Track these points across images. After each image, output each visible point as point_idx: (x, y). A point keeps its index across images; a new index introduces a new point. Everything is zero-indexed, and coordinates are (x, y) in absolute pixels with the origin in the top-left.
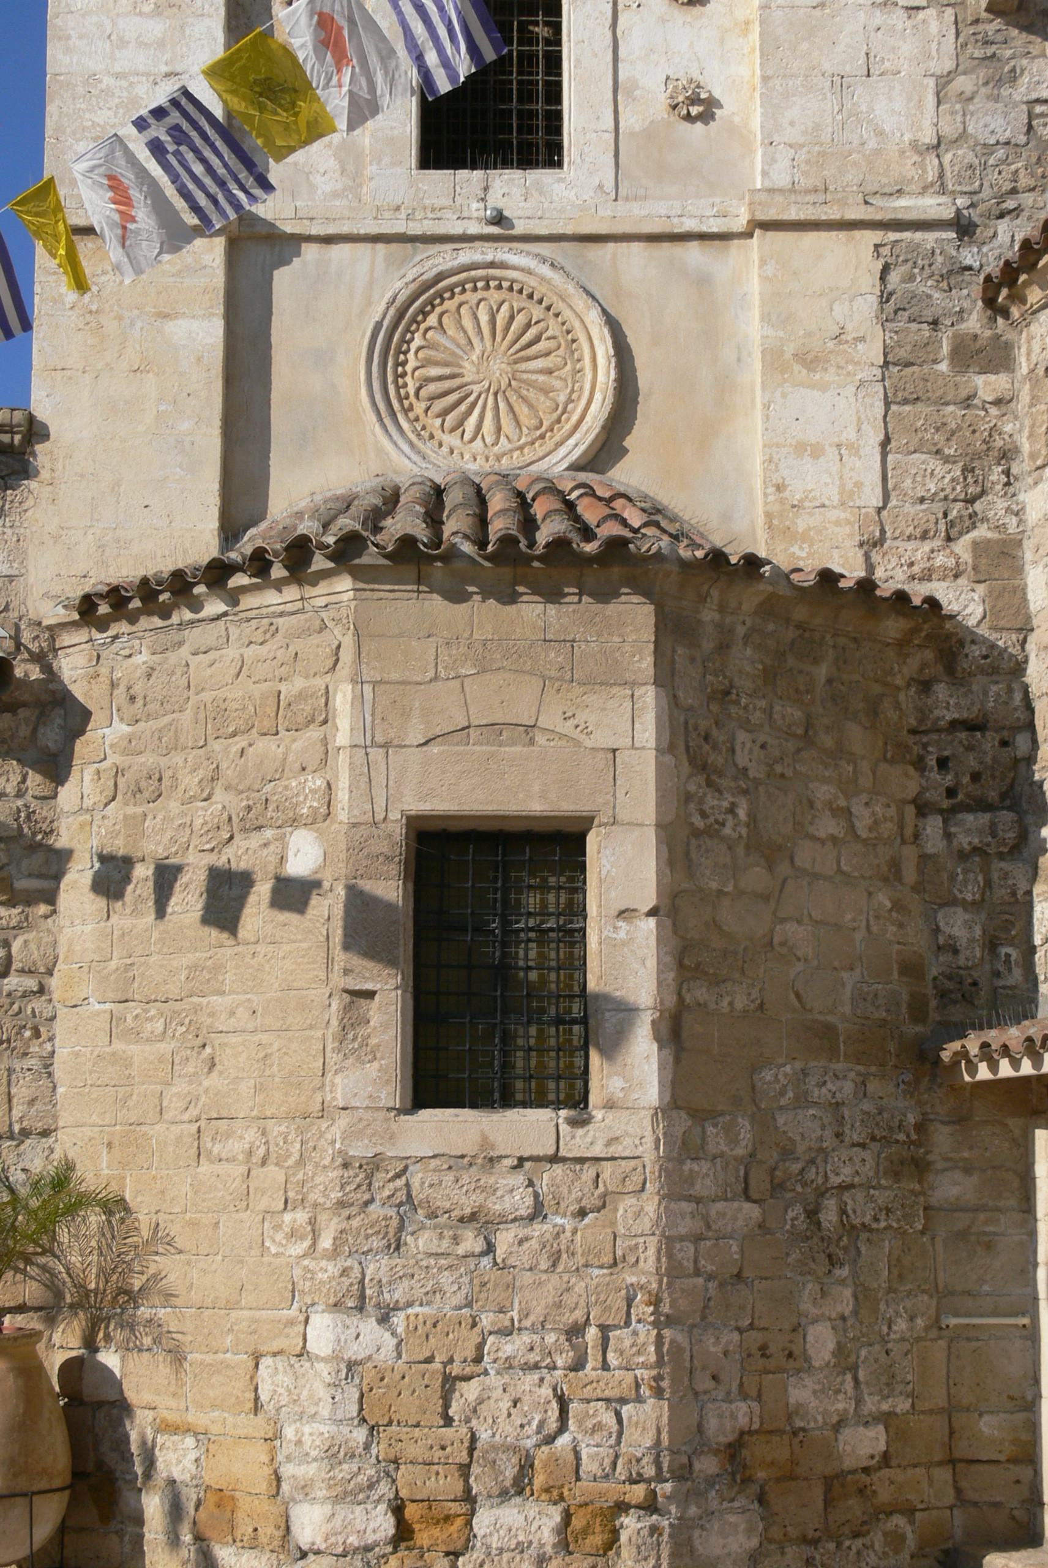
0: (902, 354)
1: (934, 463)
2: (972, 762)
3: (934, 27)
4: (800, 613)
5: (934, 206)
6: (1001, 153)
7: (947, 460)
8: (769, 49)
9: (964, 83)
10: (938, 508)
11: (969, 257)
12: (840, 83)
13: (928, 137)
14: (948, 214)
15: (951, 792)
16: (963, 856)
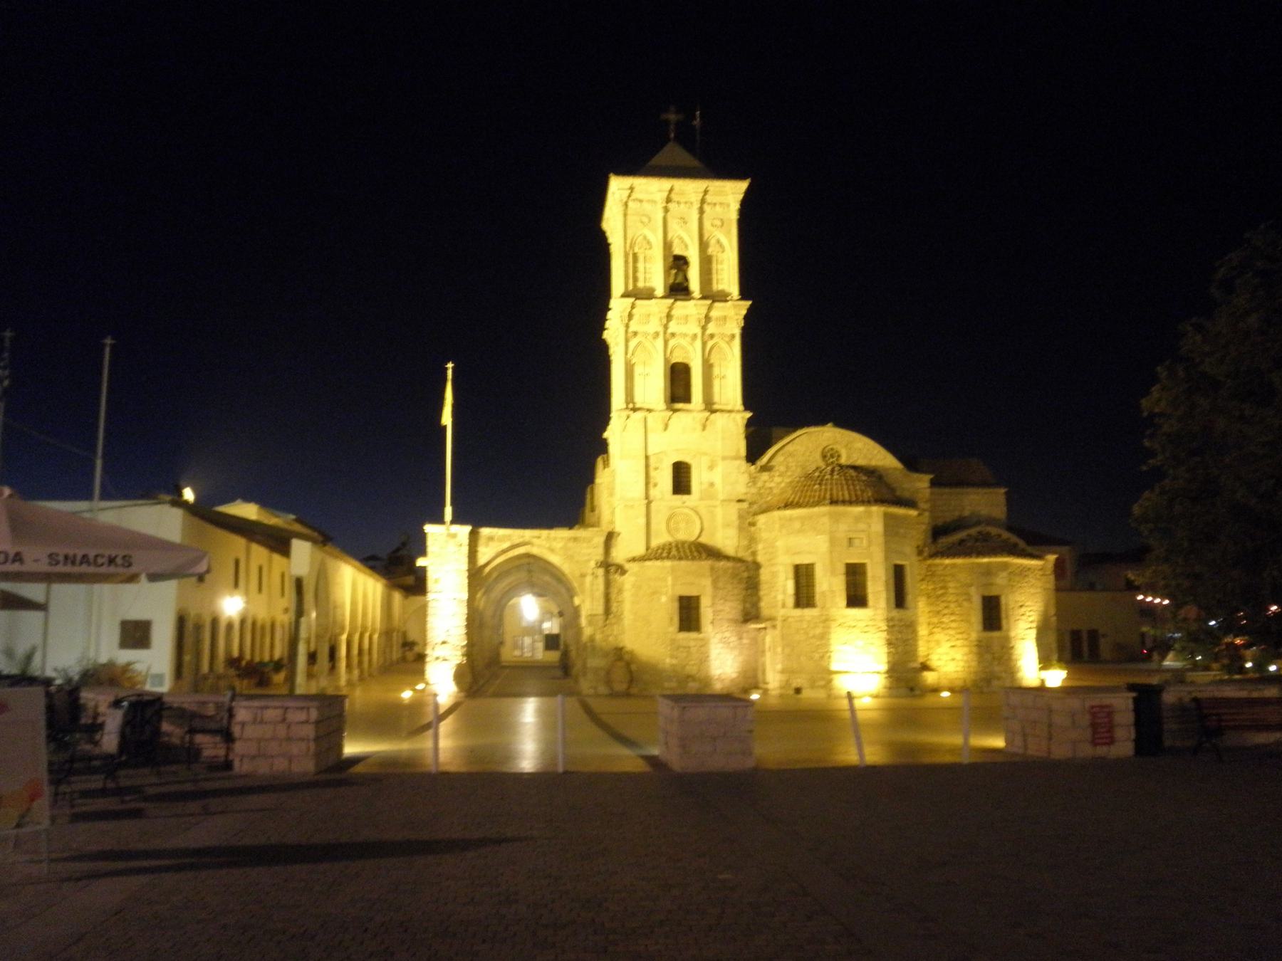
11: (751, 510)
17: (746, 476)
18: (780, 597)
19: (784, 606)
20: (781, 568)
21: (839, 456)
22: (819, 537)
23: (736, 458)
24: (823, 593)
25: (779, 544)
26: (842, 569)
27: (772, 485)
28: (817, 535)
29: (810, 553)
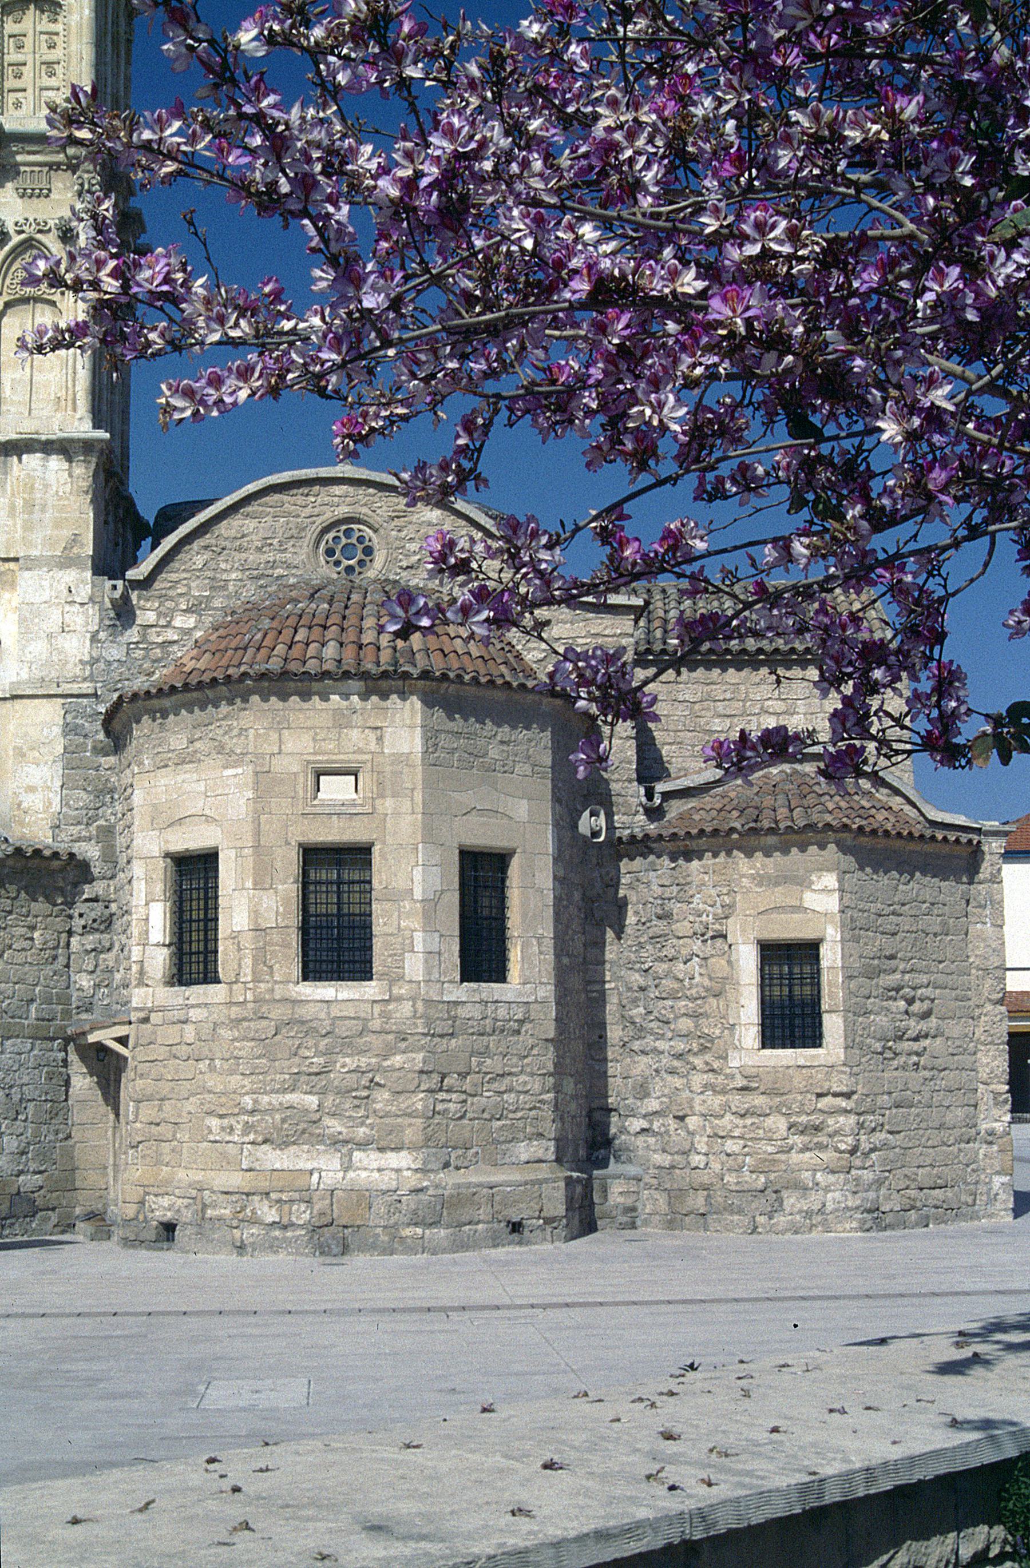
0: (71, 749)
1: (83, 794)
2: (93, 915)
3: (91, 612)
4: (10, 862)
5: (87, 687)
6: (116, 665)
7: (88, 792)
8: (22, 621)
9: (102, 635)
10: (84, 812)
12: (50, 636)
13: (87, 658)
14: (90, 691)
15: (84, 927)
16: (88, 952)
17: (92, 610)
18: (136, 953)
19: (141, 983)
20: (138, 869)
21: (368, 551)
22: (230, 772)
23: (66, 562)
24: (235, 936)
25: (138, 798)
26: (289, 862)
27: (172, 635)
28: (225, 767)
29: (209, 819)
